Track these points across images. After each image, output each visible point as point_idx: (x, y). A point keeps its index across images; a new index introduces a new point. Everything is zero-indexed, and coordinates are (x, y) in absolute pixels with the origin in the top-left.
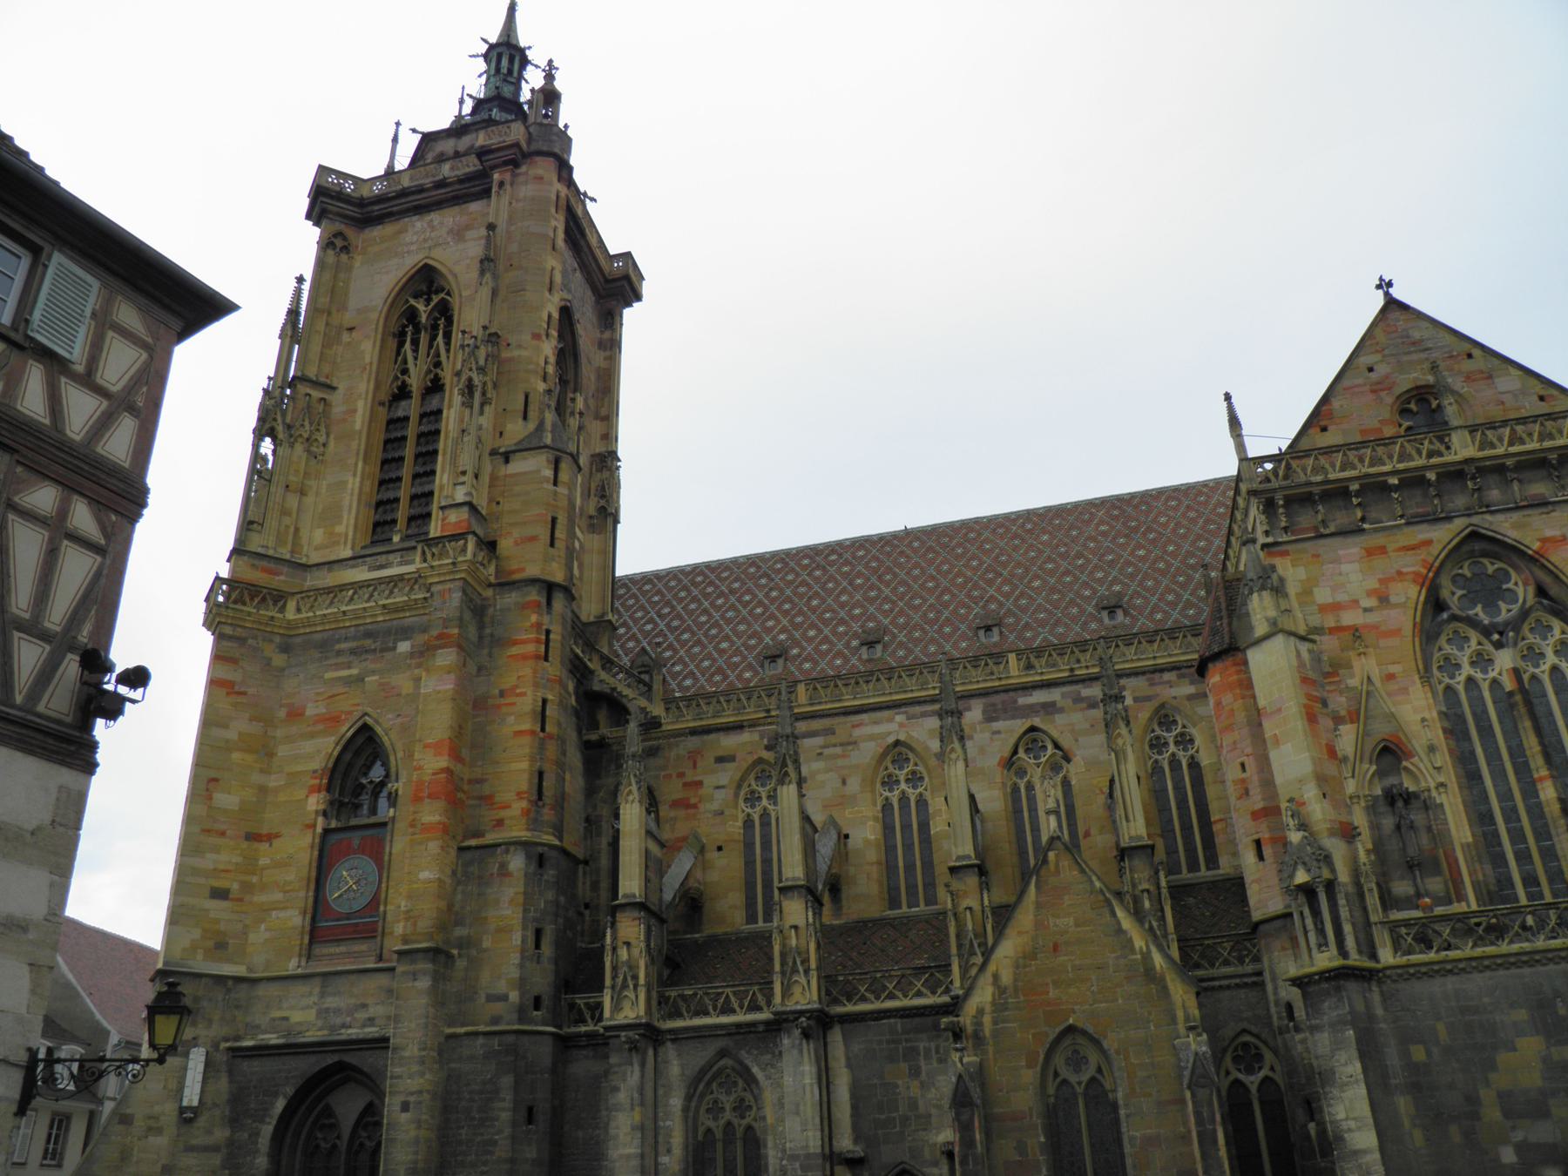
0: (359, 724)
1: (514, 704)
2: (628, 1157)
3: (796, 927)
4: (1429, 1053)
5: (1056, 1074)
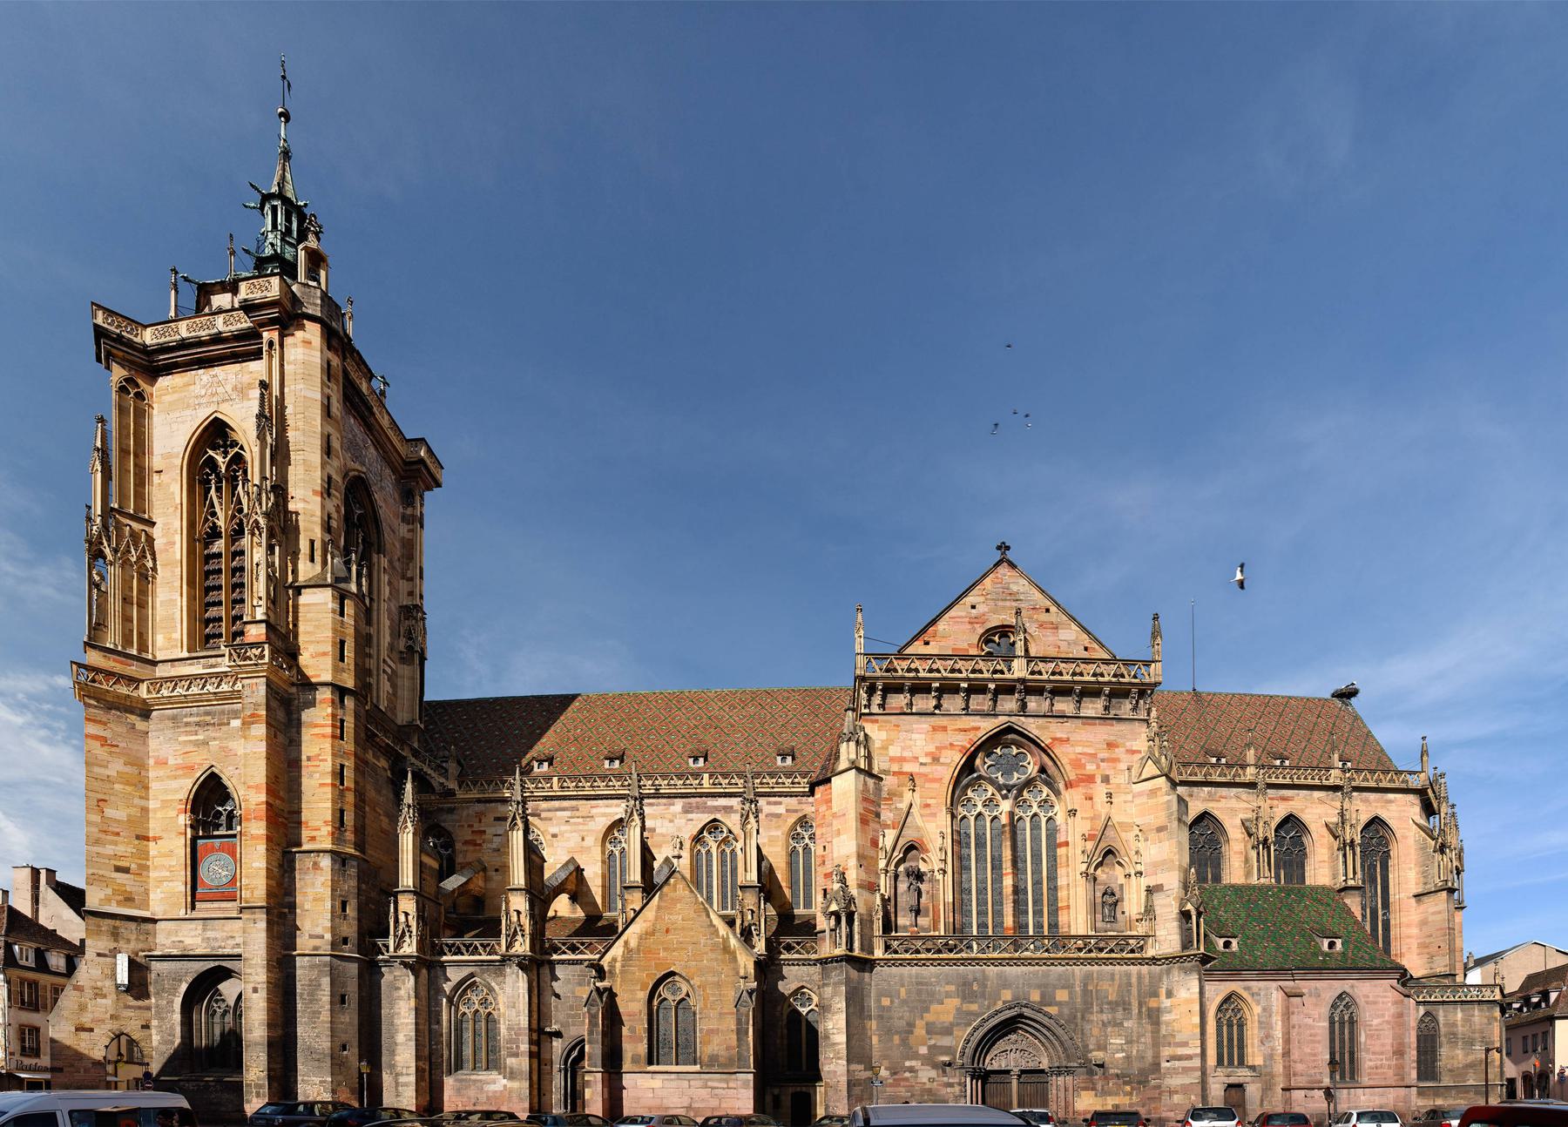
4: (892, 1002)
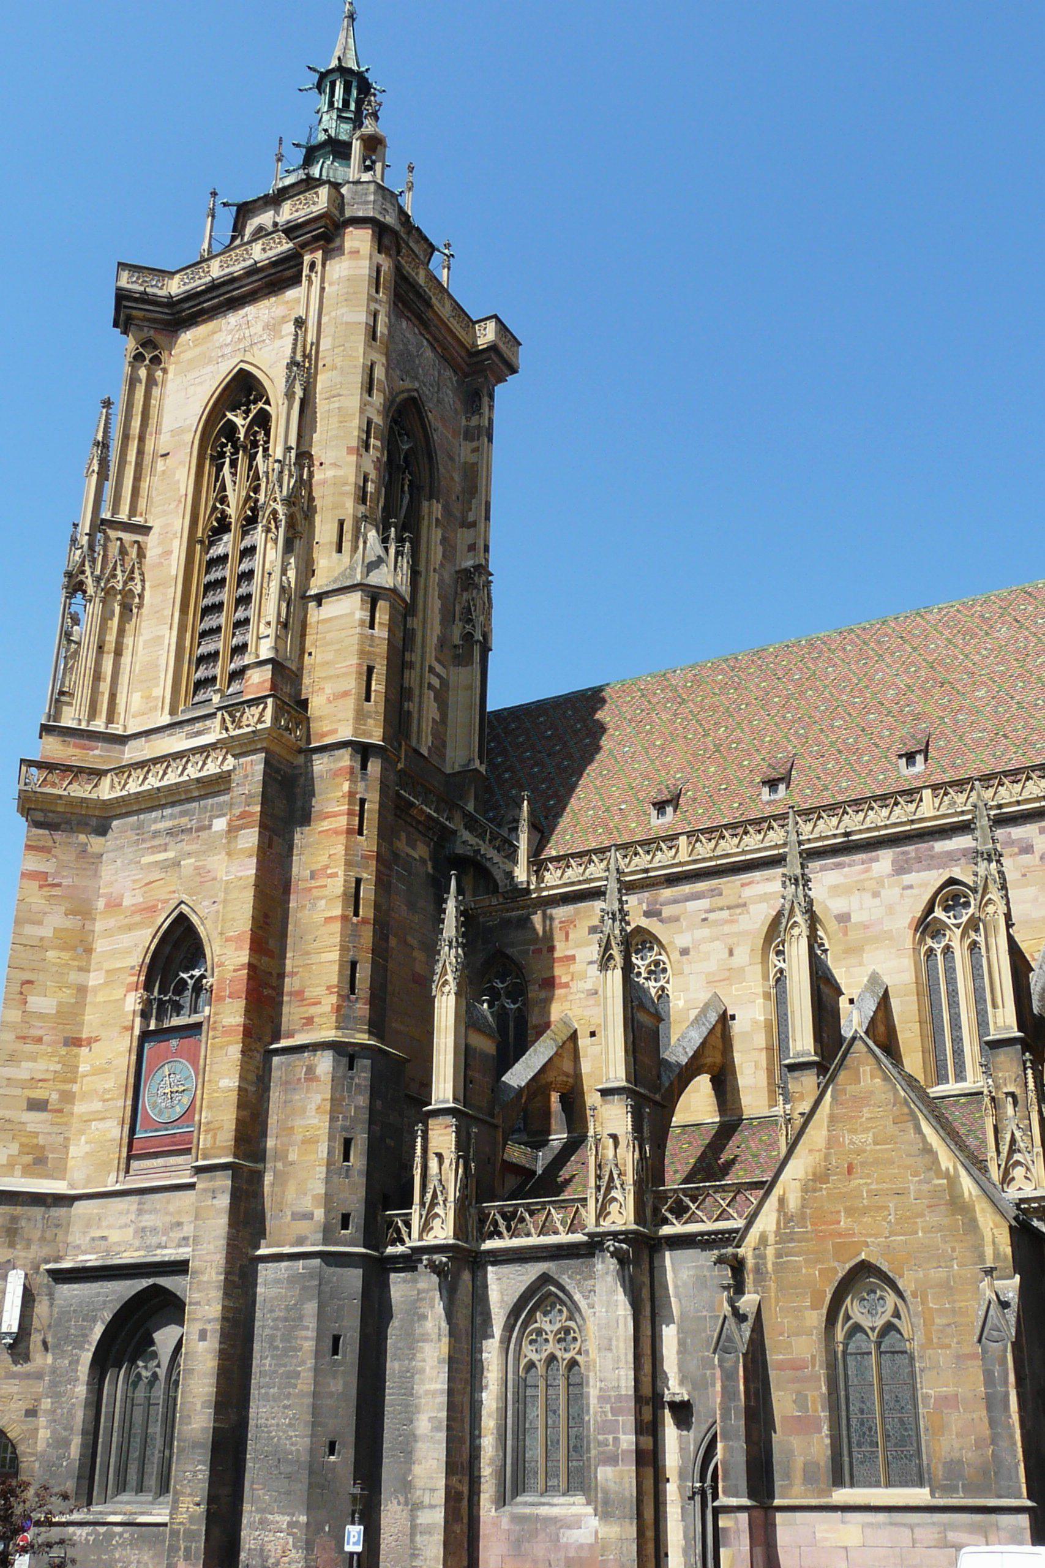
1: (325, 886)
2: (434, 1393)
3: (614, 1137)
5: (848, 1318)
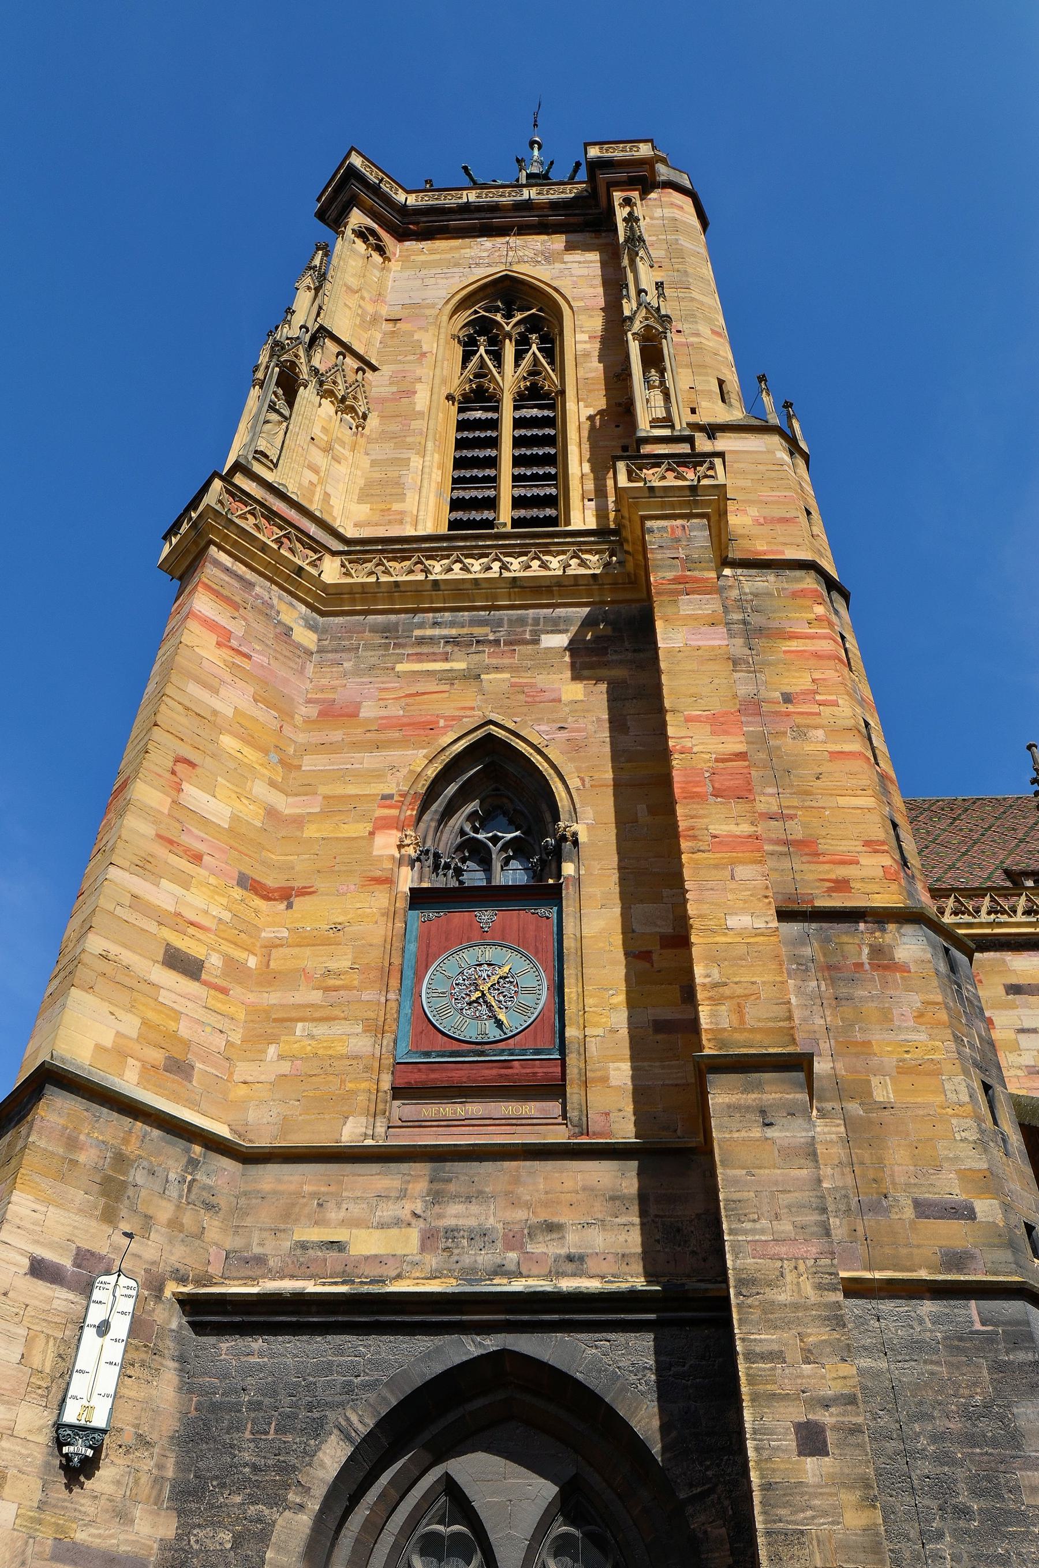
0: (479, 734)
